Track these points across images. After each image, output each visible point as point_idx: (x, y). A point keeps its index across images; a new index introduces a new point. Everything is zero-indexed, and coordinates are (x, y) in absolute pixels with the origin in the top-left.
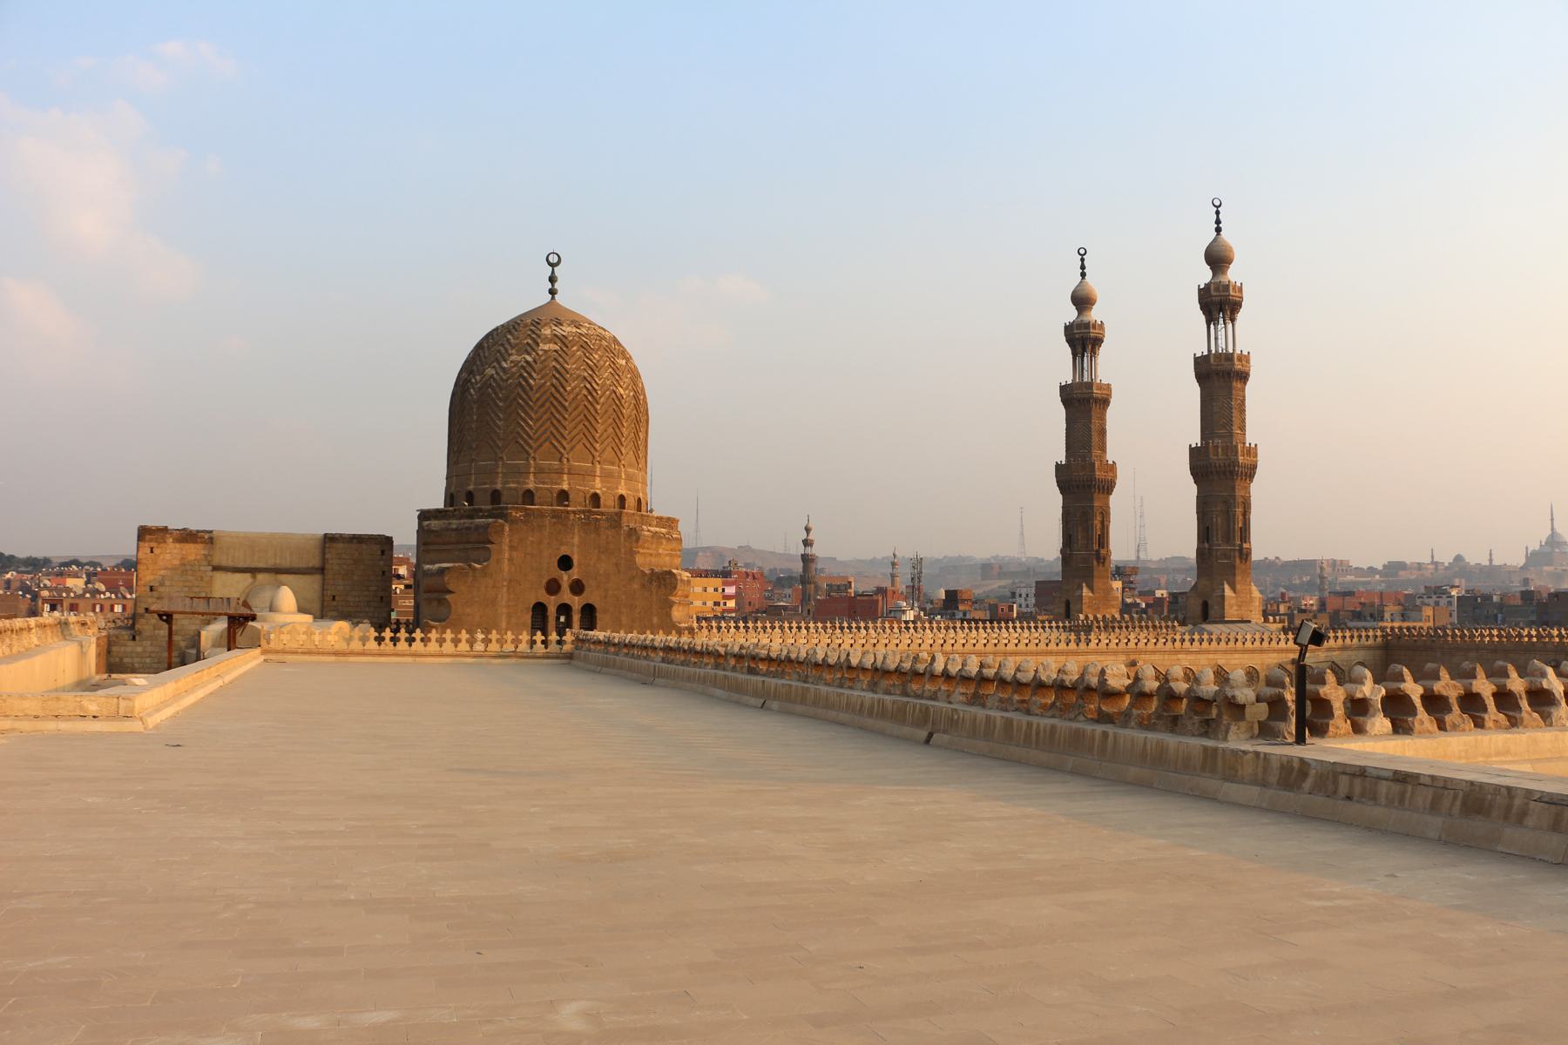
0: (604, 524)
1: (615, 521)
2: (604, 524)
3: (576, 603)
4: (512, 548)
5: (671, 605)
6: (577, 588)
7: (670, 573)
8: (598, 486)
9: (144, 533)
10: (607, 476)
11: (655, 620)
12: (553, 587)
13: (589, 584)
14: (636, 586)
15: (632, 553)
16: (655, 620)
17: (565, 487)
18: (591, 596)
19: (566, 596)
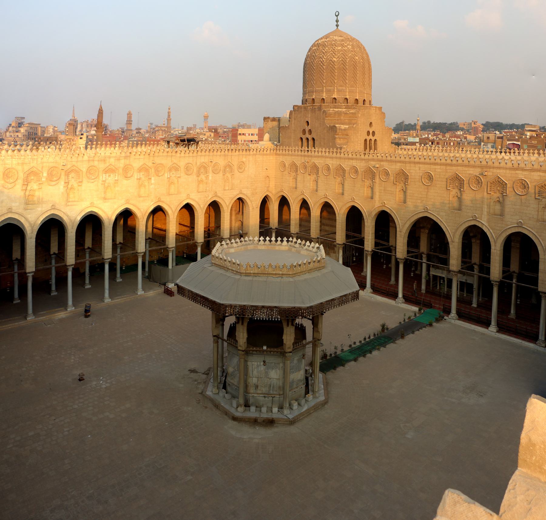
0: (317, 109)
1: (320, 108)
2: (317, 109)
3: (310, 138)
4: (295, 119)
5: (335, 138)
6: (310, 132)
7: (335, 126)
8: (324, 96)
9: (265, 119)
10: (328, 91)
11: (331, 144)
12: (304, 132)
13: (313, 131)
14: (325, 131)
15: (324, 119)
16: (331, 144)
17: (314, 97)
18: (314, 135)
19: (307, 135)
